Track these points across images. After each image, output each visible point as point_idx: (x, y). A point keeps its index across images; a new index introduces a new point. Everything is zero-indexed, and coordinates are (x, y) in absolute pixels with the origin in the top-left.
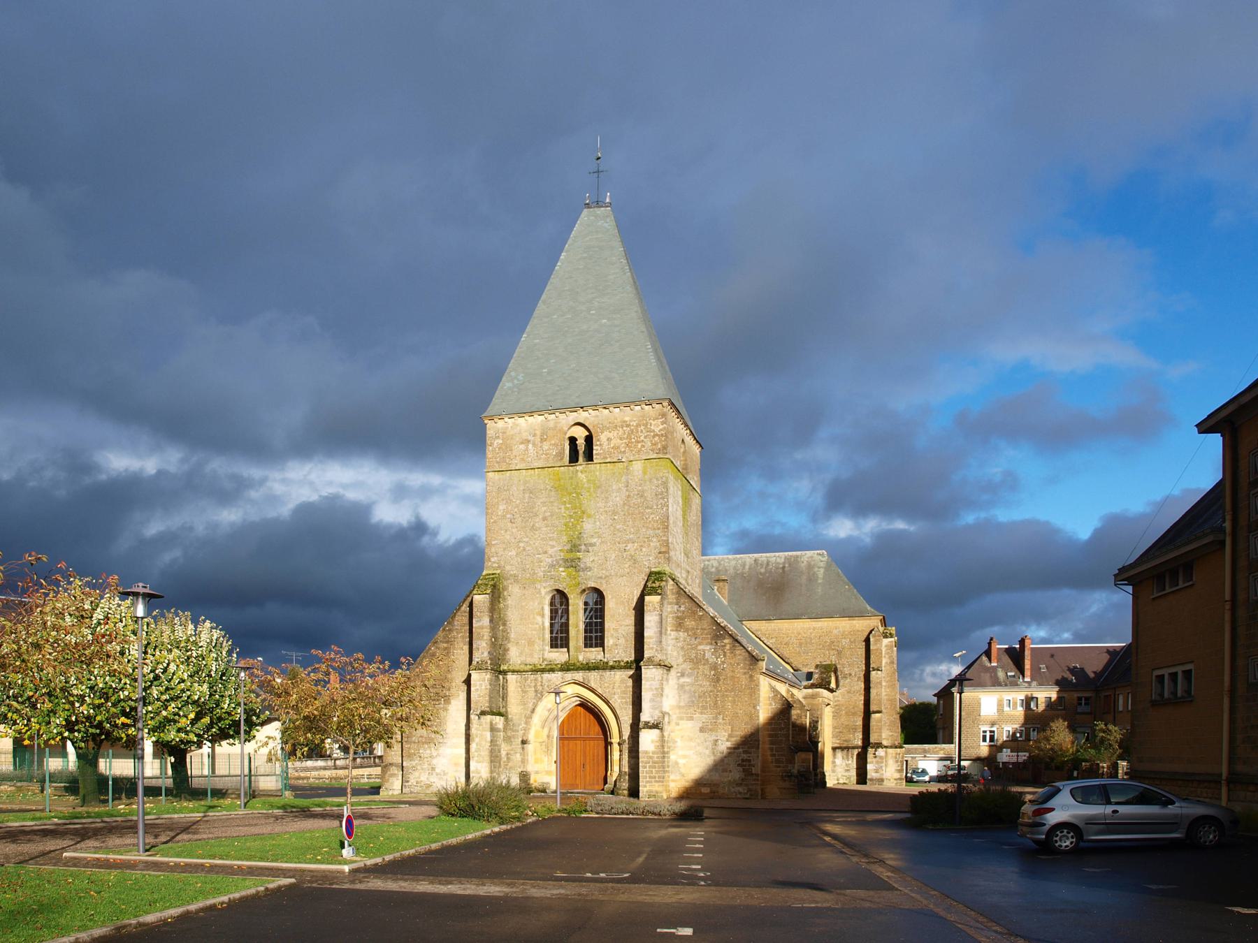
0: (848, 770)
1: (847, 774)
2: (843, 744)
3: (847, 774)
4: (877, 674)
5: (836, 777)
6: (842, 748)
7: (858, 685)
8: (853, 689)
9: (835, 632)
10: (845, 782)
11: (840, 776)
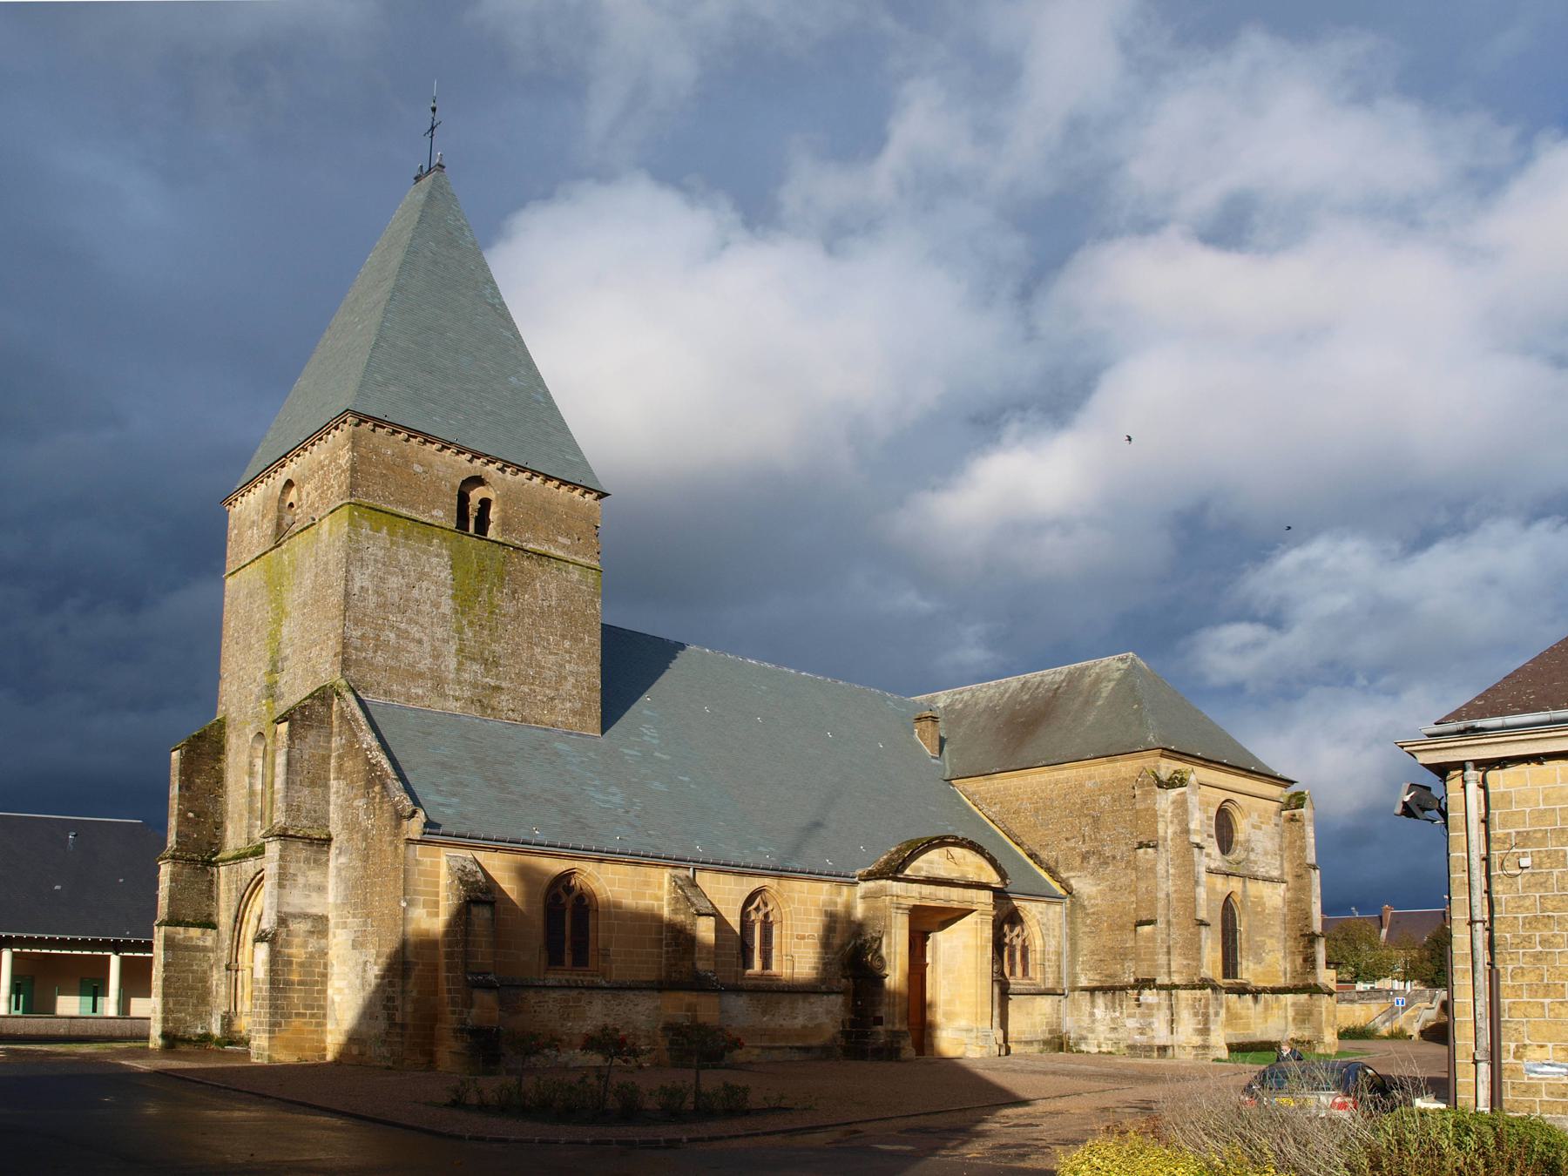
0: (1115, 1029)
1: (1112, 1036)
2: (1104, 982)
3: (1112, 1036)
4: (1146, 853)
5: (1096, 1042)
6: (1105, 990)
7: (1126, 875)
8: (1118, 884)
9: (1089, 784)
10: (1110, 1049)
11: (1102, 1040)
